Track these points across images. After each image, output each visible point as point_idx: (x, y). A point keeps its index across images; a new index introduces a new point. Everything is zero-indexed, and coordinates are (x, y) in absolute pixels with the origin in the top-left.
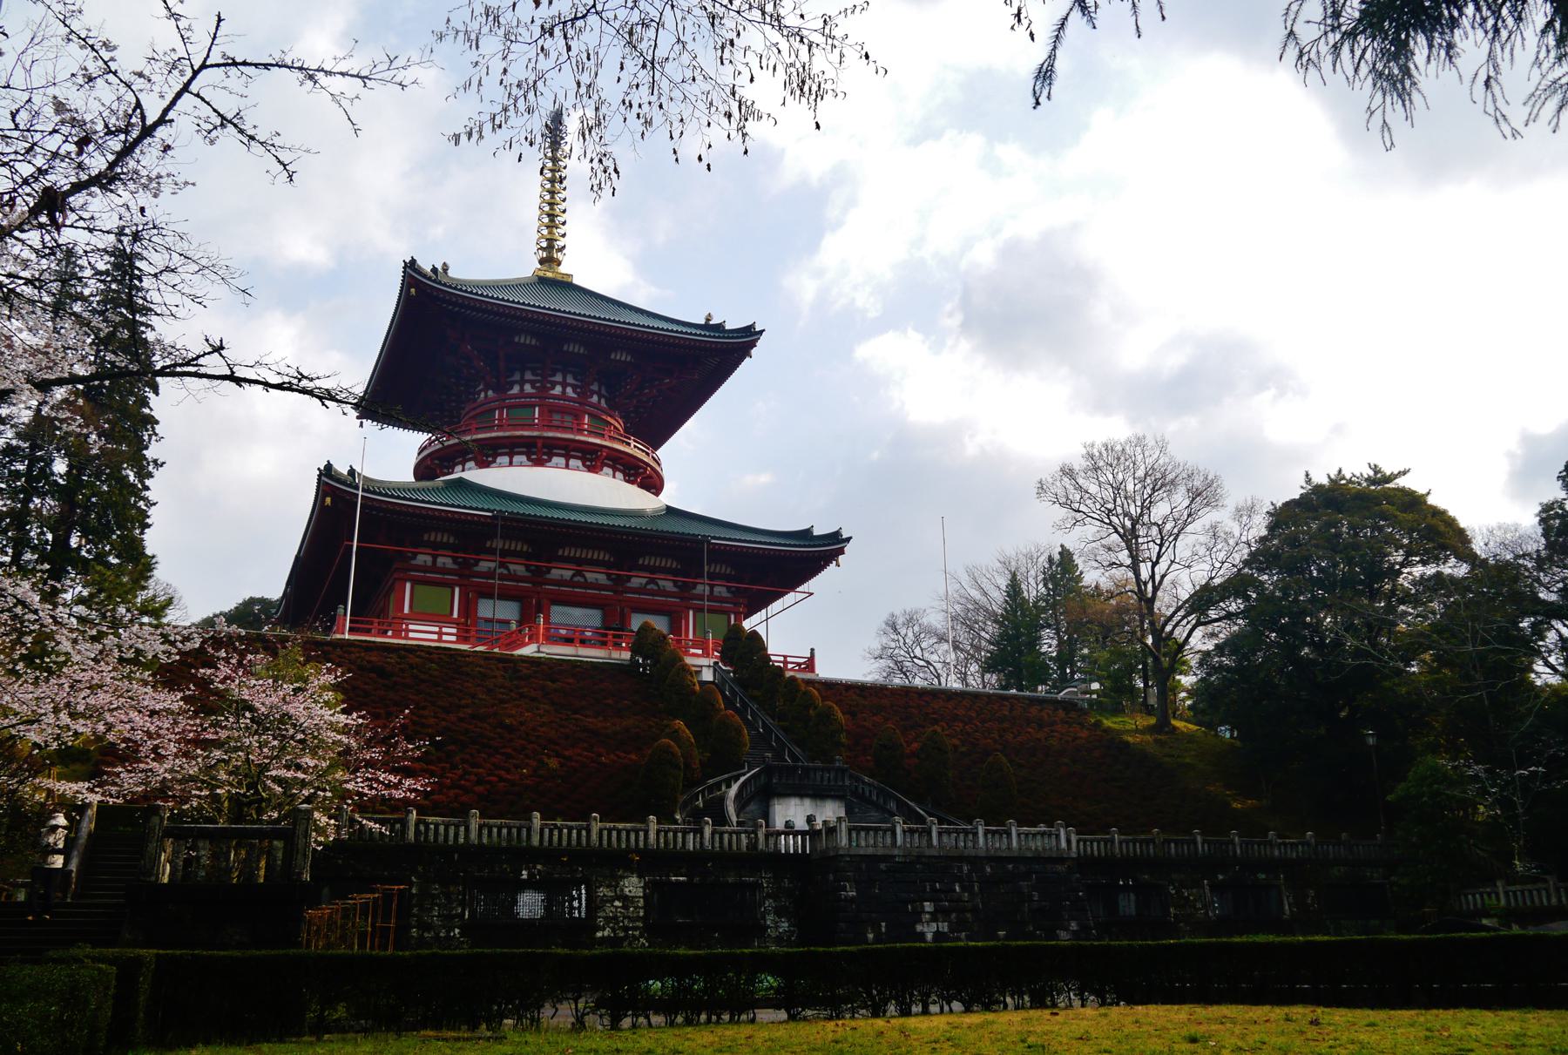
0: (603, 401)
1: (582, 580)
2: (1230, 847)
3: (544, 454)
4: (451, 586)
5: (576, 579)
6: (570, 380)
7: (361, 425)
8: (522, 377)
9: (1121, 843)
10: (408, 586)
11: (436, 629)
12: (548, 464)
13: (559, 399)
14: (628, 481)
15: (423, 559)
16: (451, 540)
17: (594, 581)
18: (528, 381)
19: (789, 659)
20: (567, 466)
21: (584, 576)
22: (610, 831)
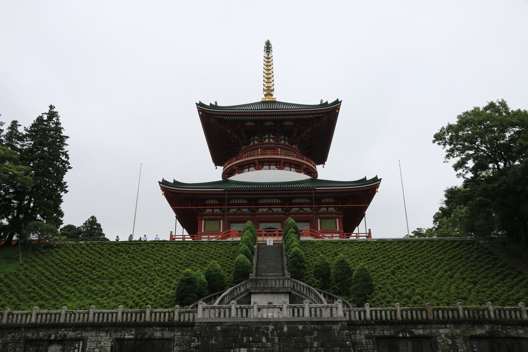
0: (286, 143)
2: (486, 312)
4: (219, 220)
5: (269, 212)
6: (271, 136)
7: (216, 168)
8: (254, 139)
9: (402, 311)
10: (203, 222)
12: (262, 169)
13: (267, 144)
14: (297, 172)
15: (209, 211)
16: (217, 202)
18: (256, 140)
20: (270, 169)
21: (272, 210)
22: (99, 314)
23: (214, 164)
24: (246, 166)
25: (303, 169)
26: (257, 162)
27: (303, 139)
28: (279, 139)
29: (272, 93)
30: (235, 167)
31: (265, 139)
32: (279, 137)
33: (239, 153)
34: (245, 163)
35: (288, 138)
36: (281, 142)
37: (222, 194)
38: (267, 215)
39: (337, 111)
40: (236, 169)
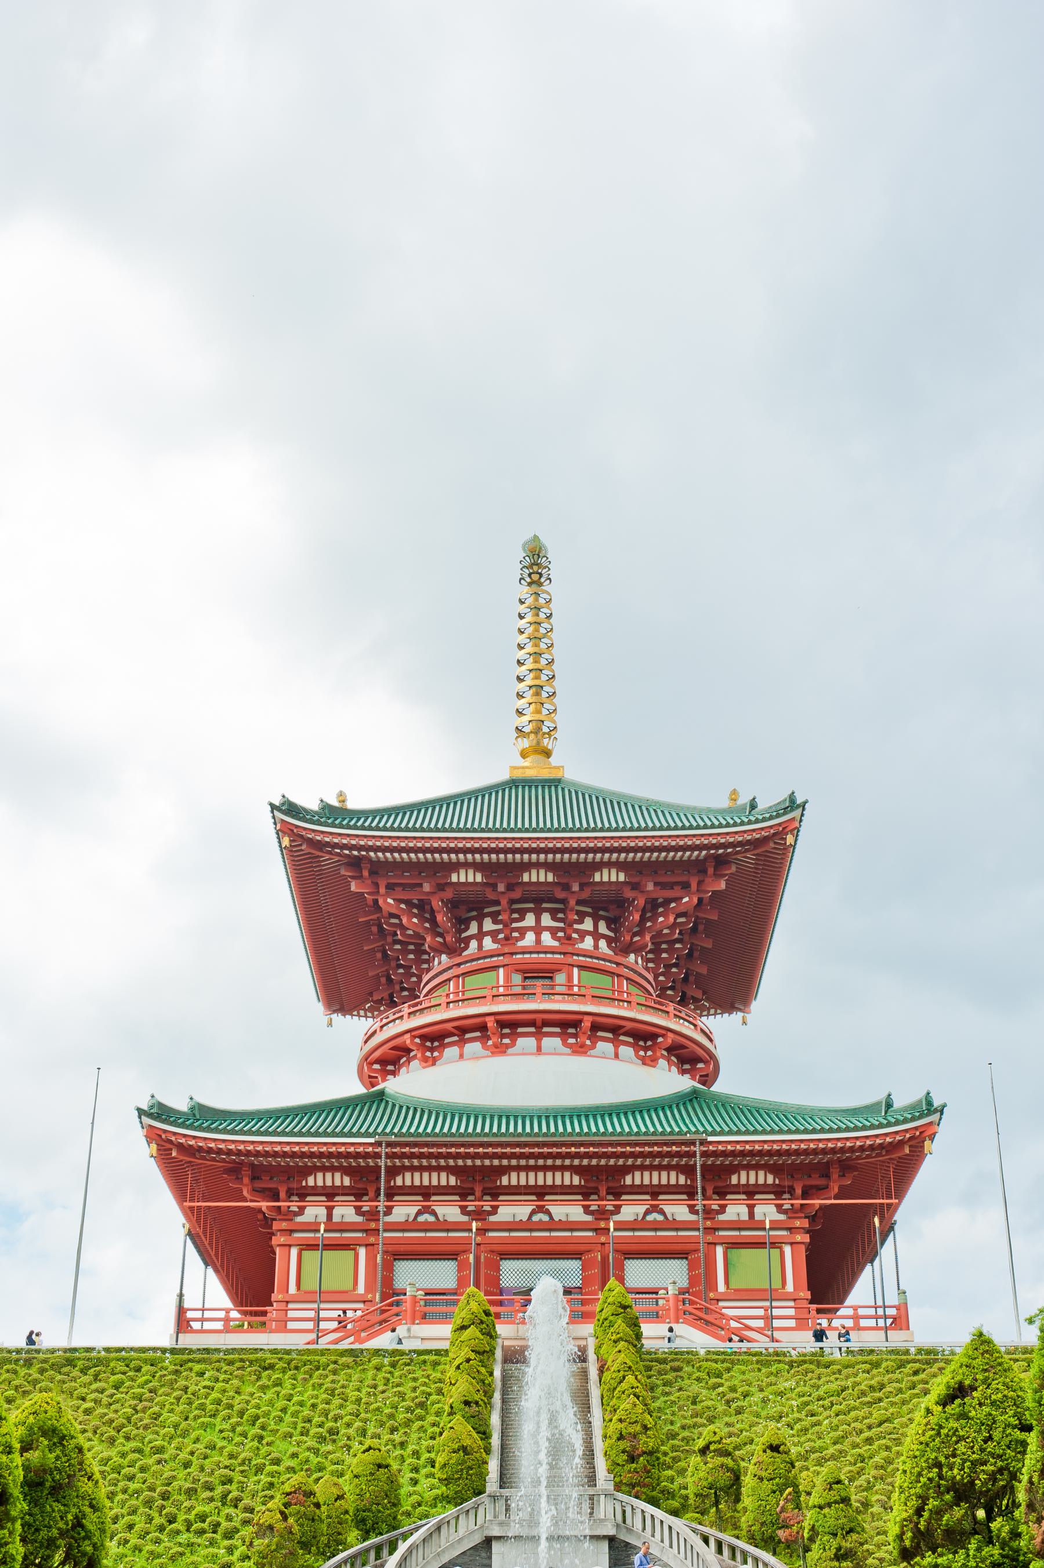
0: (602, 943)
1: (545, 1218)
3: (503, 1036)
5: (536, 1218)
6: (546, 920)
7: (330, 1024)
8: (480, 927)
11: (311, 1314)
12: (510, 1051)
13: (531, 953)
17: (564, 1219)
18: (488, 933)
19: (861, 1312)
23: (320, 1007)
24: (452, 1035)
25: (668, 1050)
26: (491, 1023)
27: (666, 931)
28: (577, 931)
29: (550, 747)
30: (408, 1042)
31: (523, 932)
32: (576, 926)
33: (425, 980)
34: (449, 1026)
35: (609, 928)
36: (581, 946)
37: (366, 1156)
38: (531, 1230)
39: (790, 839)
40: (411, 1047)
